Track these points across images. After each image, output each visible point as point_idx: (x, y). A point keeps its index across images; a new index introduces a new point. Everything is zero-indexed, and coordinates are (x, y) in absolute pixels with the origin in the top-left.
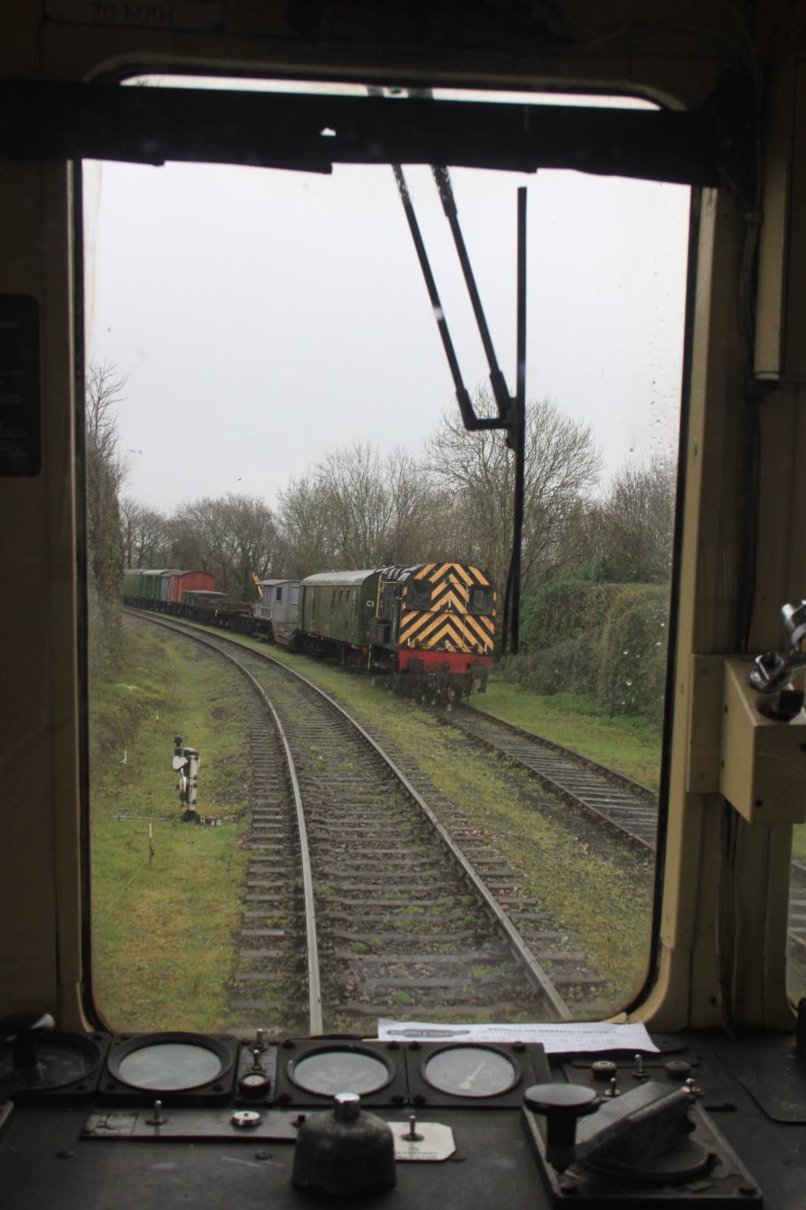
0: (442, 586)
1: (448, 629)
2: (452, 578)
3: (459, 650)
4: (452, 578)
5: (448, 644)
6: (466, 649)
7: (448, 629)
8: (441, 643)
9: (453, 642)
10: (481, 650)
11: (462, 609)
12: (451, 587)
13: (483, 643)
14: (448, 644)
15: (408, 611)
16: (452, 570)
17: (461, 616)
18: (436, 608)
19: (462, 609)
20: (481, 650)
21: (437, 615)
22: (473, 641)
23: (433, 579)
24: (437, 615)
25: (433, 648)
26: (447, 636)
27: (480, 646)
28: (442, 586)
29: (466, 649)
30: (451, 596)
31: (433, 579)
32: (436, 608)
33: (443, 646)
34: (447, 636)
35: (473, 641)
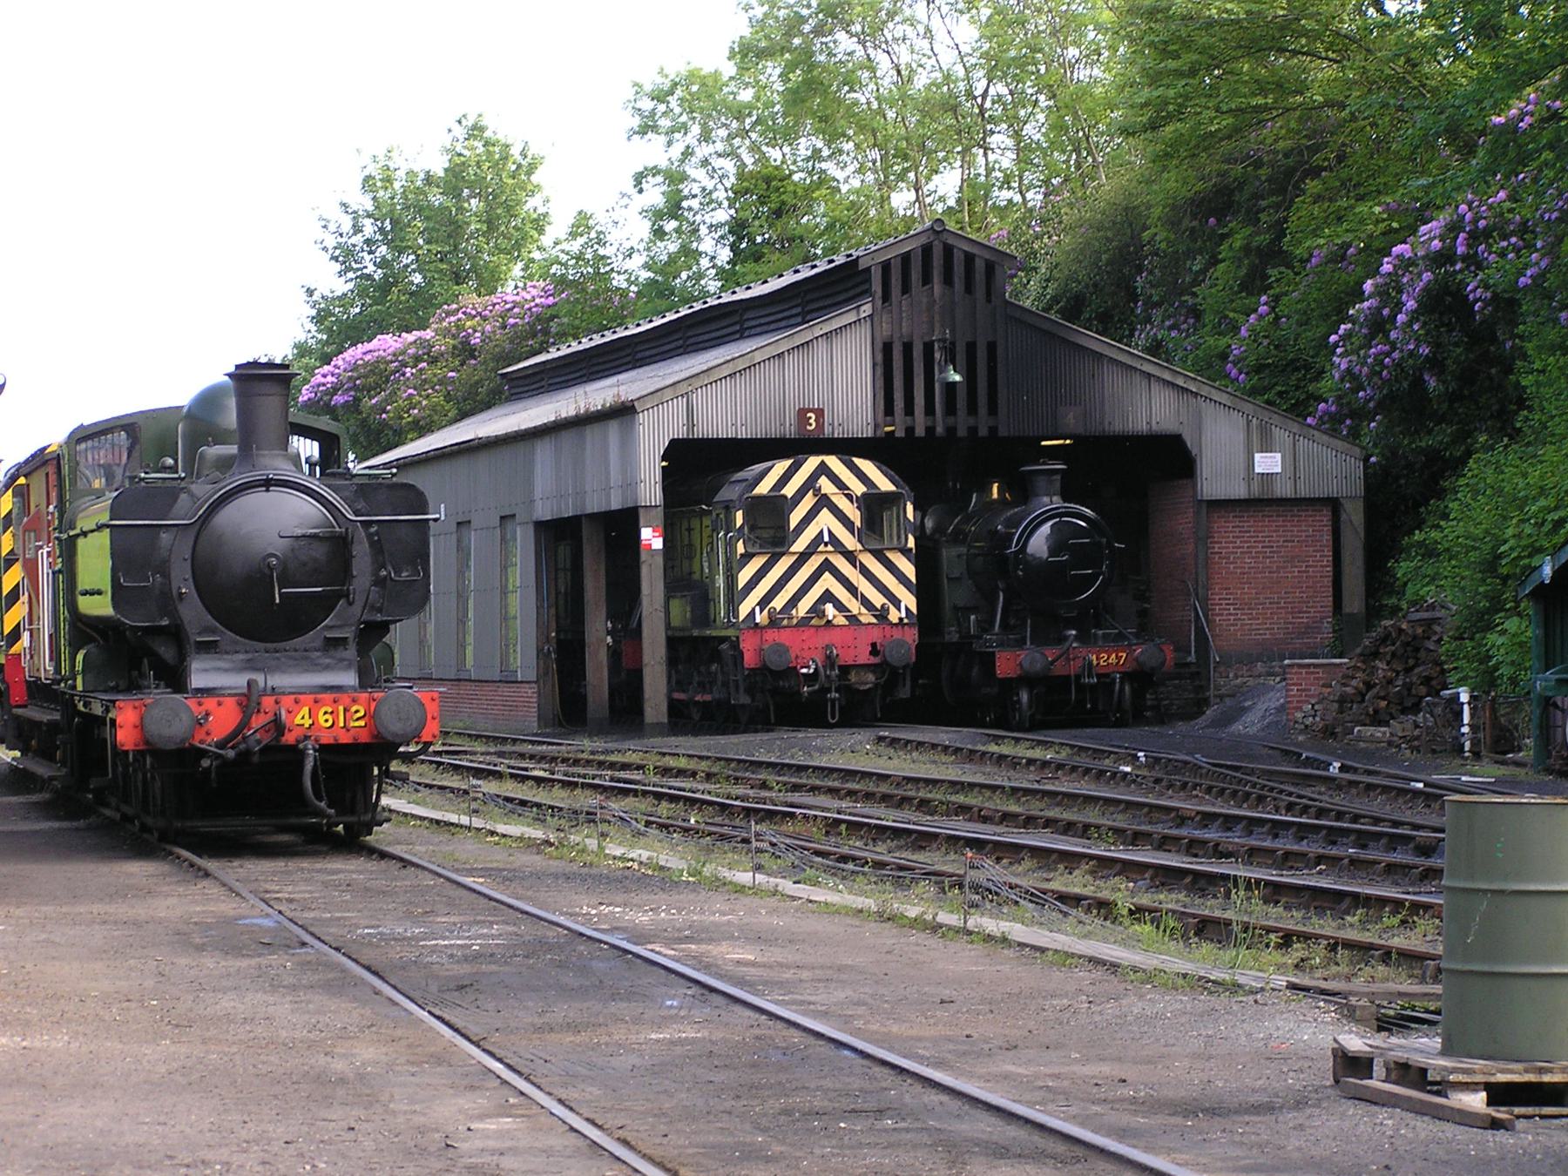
0: (808, 501)
1: (827, 582)
2: (825, 484)
3: (853, 619)
4: (825, 484)
5: (830, 609)
6: (867, 618)
7: (827, 582)
8: (817, 610)
9: (840, 606)
10: (894, 616)
11: (850, 542)
12: (824, 502)
13: (896, 602)
14: (830, 609)
15: (748, 557)
16: (823, 469)
17: (850, 557)
18: (800, 545)
19: (850, 542)
20: (894, 616)
21: (803, 557)
22: (878, 600)
23: (789, 490)
24: (803, 557)
25: (804, 622)
26: (828, 596)
27: (892, 609)
28: (808, 501)
29: (867, 618)
30: (825, 519)
31: (789, 490)
32: (800, 545)
33: (823, 614)
34: (828, 596)
35: (878, 600)
